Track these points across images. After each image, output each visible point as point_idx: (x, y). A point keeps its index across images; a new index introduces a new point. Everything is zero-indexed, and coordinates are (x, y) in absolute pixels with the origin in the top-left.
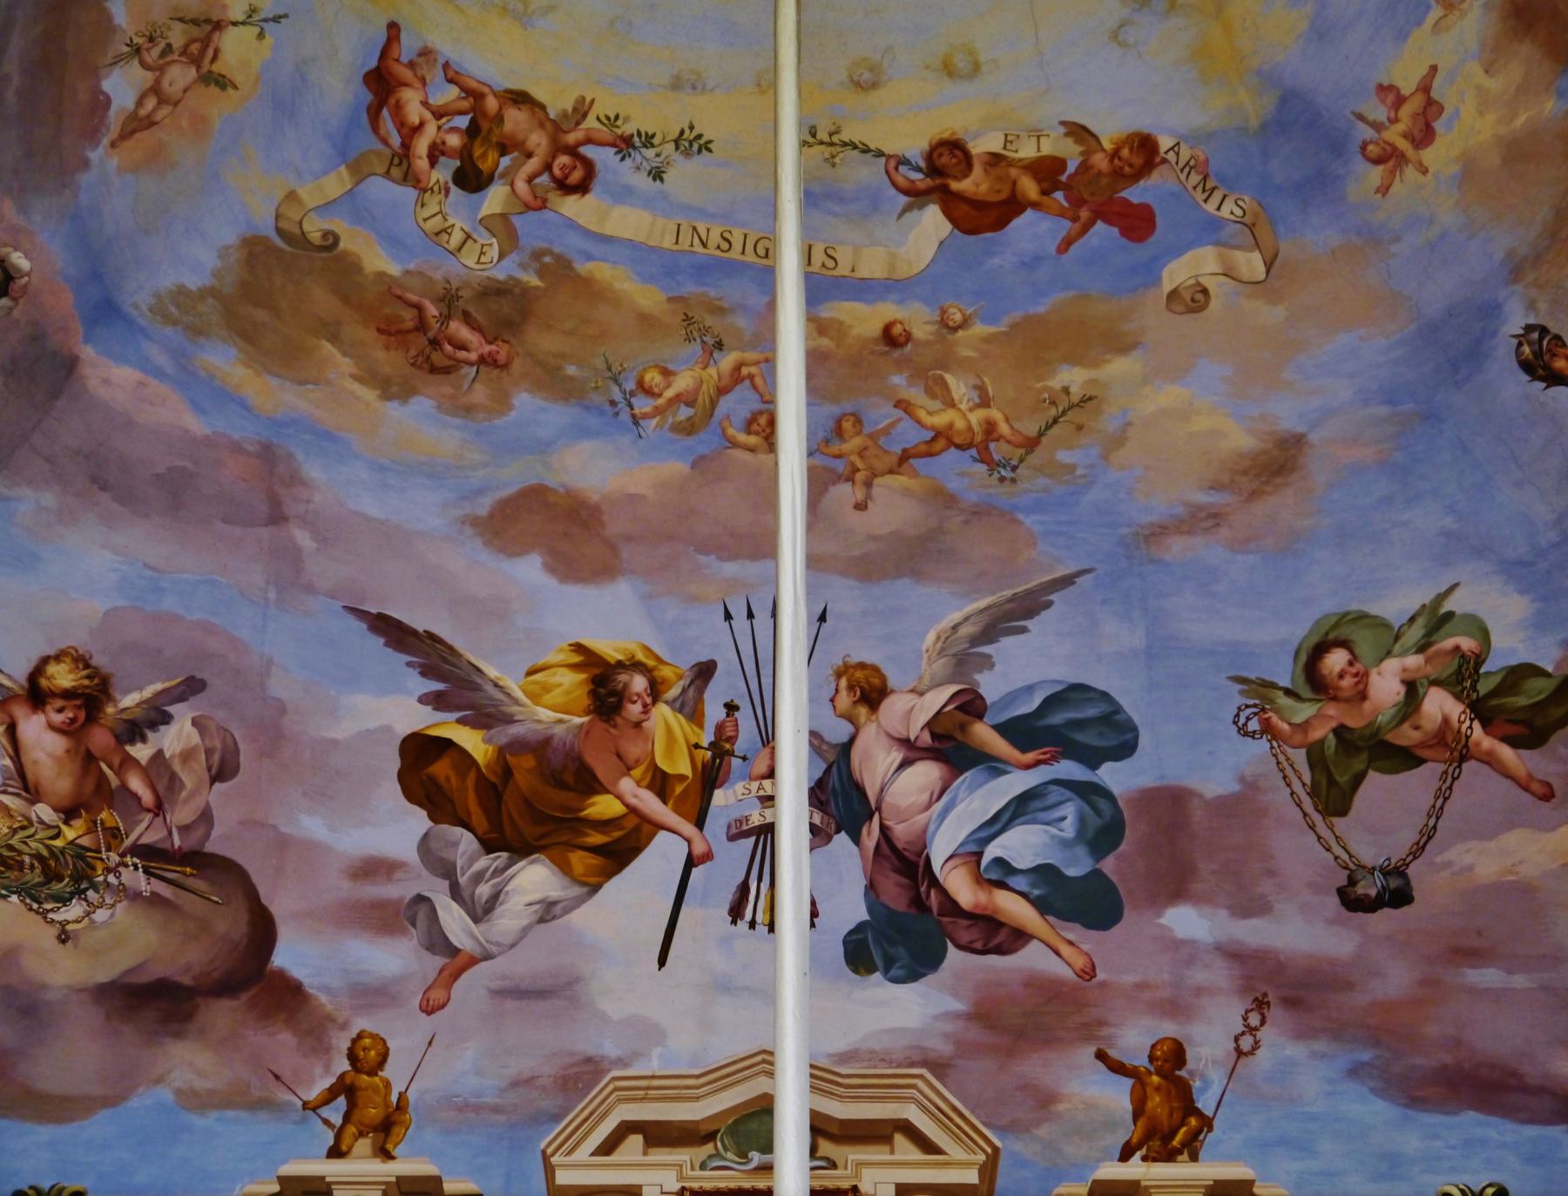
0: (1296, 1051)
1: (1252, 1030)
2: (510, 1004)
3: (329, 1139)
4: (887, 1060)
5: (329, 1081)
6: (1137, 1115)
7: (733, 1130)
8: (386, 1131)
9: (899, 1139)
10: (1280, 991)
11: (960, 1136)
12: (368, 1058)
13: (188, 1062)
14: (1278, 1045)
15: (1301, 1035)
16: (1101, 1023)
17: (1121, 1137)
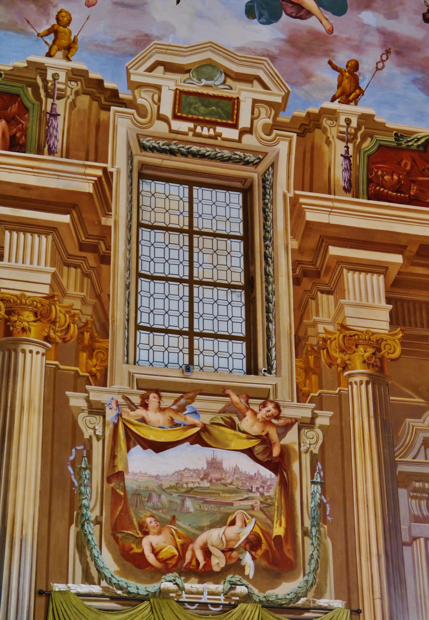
0: (396, 71)
1: (383, 61)
2: (120, 9)
3: (47, 50)
4: (254, 53)
5: (48, 27)
6: (339, 85)
7: (197, 70)
8: (69, 49)
9: (255, 82)
10: (395, 48)
11: (277, 84)
12: (63, 20)
15: (400, 65)
16: (332, 51)
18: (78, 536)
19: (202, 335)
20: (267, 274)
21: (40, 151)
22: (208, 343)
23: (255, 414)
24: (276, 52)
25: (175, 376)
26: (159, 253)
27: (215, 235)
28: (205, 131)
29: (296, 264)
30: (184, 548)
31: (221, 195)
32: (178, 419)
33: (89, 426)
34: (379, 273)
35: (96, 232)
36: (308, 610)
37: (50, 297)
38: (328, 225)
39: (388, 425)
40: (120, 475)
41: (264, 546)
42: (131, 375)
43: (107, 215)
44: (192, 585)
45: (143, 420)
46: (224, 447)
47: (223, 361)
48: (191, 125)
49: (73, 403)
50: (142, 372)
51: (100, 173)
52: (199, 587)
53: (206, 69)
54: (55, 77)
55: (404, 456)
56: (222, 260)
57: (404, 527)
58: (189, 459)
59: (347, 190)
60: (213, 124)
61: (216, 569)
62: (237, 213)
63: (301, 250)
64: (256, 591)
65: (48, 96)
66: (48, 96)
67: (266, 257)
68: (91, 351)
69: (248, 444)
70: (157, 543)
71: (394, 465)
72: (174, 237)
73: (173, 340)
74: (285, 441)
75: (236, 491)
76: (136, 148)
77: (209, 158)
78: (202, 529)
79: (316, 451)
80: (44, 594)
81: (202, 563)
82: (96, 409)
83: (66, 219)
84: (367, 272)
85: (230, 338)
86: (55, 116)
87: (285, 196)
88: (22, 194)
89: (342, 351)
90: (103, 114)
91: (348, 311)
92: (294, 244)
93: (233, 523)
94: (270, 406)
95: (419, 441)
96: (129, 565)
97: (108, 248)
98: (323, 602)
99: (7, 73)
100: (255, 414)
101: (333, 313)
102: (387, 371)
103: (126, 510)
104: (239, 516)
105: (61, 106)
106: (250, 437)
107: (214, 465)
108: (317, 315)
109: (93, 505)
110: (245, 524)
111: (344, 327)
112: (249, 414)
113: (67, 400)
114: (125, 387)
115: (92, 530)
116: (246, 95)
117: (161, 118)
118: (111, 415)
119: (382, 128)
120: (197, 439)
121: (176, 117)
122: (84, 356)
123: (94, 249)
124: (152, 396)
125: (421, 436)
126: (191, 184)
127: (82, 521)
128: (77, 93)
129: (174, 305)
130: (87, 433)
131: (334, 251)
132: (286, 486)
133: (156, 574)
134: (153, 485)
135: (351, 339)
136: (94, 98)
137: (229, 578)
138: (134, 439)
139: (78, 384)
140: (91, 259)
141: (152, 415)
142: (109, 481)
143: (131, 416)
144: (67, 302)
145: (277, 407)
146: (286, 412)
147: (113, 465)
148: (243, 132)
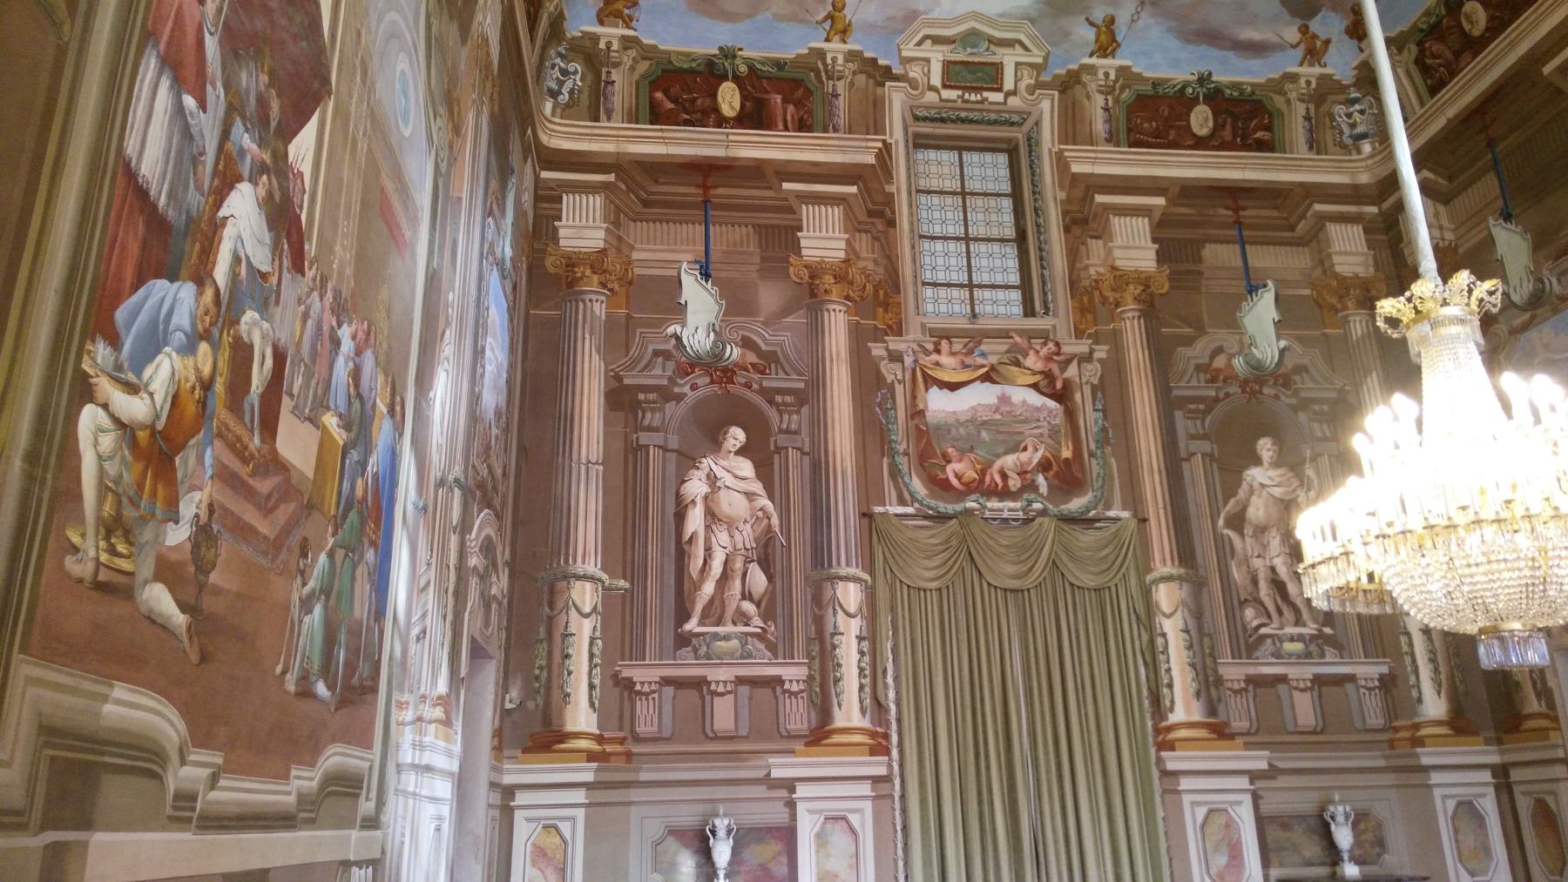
0: (1151, 21)
8: (844, 33)
11: (1039, 47)
14: (1146, 20)
17: (1090, 49)
18: (890, 466)
19: (980, 286)
20: (1038, 226)
21: (825, 130)
22: (987, 294)
24: (1034, 14)
25: (964, 324)
26: (937, 215)
27: (985, 195)
28: (973, 97)
29: (1065, 213)
30: (983, 473)
31: (988, 157)
32: (968, 361)
33: (890, 371)
35: (879, 198)
36: (1099, 520)
37: (846, 261)
38: (1092, 175)
39: (1161, 355)
40: (922, 413)
41: (1055, 468)
42: (923, 326)
44: (994, 504)
45: (937, 364)
46: (1010, 382)
47: (1004, 307)
48: (960, 93)
49: (875, 352)
50: (933, 322)
51: (880, 145)
52: (1000, 505)
53: (971, 38)
54: (834, 59)
55: (1180, 380)
56: (994, 217)
57: (1182, 445)
59: (1108, 141)
61: (1013, 489)
62: (1004, 172)
63: (1068, 201)
65: (830, 78)
67: (1036, 210)
68: (886, 306)
70: (958, 469)
72: (949, 200)
73: (955, 293)
74: (1067, 374)
75: (1026, 421)
76: (910, 119)
78: (998, 456)
79: (1096, 382)
80: (867, 515)
81: (1000, 485)
82: (896, 357)
83: (853, 189)
85: (1007, 287)
86: (836, 96)
88: (814, 170)
89: (1114, 290)
90: (879, 90)
91: (1117, 253)
92: (1062, 195)
93: (1025, 449)
94: (1051, 345)
95: (1191, 368)
97: (893, 213)
98: (1112, 514)
99: (792, 61)
100: (1037, 352)
103: (929, 443)
104: (1029, 442)
105: (841, 86)
106: (1034, 373)
107: (1004, 399)
110: (1036, 450)
111: (1114, 268)
112: (1032, 353)
113: (869, 351)
114: (919, 336)
115: (902, 462)
116: (1009, 60)
117: (932, 88)
118: (908, 361)
119: (1139, 78)
120: (987, 378)
121: (945, 86)
122: (881, 310)
123: (881, 214)
124: (944, 342)
125: (1193, 362)
126: (960, 150)
127: (892, 453)
128: (854, 73)
129: (953, 261)
130: (890, 378)
131: (1100, 198)
132: (1070, 414)
134: (951, 420)
135: (1121, 279)
136: (870, 76)
137: (1025, 496)
138: (930, 381)
139: (878, 335)
140: (878, 222)
141: (945, 359)
142: (913, 417)
143: (927, 360)
144: (861, 264)
145: (1057, 344)
146: (1066, 349)
147: (914, 405)
148: (1008, 94)
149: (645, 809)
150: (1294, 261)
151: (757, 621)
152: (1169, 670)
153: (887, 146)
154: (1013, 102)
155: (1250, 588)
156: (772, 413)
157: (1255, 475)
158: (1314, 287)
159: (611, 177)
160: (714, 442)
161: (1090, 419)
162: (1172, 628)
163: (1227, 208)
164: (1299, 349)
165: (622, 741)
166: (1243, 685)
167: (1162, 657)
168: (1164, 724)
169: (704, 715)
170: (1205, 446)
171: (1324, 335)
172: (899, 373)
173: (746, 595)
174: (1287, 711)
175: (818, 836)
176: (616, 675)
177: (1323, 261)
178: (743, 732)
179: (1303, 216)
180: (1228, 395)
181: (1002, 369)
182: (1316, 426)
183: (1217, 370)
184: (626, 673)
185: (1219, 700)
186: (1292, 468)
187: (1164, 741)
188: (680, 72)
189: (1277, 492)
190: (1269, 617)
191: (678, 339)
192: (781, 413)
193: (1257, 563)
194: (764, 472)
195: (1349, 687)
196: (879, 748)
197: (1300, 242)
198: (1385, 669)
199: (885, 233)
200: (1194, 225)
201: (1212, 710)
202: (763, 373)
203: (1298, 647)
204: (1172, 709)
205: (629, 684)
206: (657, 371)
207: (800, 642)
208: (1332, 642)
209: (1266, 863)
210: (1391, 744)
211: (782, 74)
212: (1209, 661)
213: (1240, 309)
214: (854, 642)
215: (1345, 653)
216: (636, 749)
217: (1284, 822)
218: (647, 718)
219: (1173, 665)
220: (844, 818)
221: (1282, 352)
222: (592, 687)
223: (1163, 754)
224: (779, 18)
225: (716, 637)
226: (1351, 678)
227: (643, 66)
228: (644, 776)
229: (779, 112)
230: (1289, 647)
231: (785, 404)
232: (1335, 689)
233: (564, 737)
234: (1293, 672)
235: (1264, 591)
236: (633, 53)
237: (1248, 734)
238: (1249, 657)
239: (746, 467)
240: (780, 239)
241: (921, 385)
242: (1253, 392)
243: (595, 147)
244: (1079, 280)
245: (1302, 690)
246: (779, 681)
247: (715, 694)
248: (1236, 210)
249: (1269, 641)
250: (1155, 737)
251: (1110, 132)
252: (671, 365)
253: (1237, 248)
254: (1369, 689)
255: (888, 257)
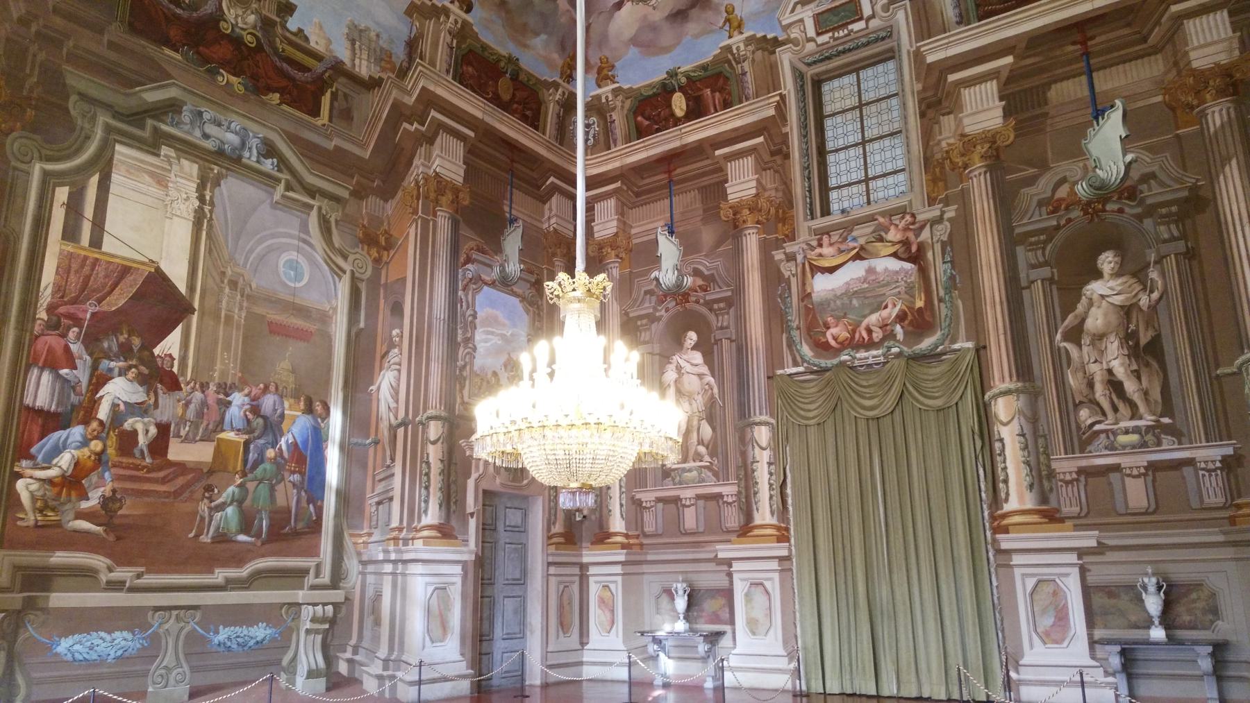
12: (730, 10)
13: (692, 27)
21: (741, 102)
22: (880, 183)
23: (897, 226)
28: (841, 33)
29: (920, 102)
30: (854, 331)
31: (880, 68)
32: (843, 247)
33: (787, 269)
34: (992, 79)
37: (757, 195)
39: (1004, 200)
40: (809, 295)
42: (809, 228)
43: (785, 125)
44: (862, 354)
45: (820, 255)
46: (876, 256)
48: (830, 34)
49: (777, 258)
51: (778, 98)
52: (866, 354)
54: (738, 49)
55: (1022, 219)
57: (1023, 275)
58: (853, 272)
59: (959, 23)
60: (845, 25)
63: (924, 89)
64: (905, 349)
65: (738, 63)
66: (738, 63)
69: (892, 250)
71: (1013, 229)
75: (888, 284)
77: (854, 49)
78: (865, 317)
79: (945, 238)
82: (791, 258)
83: (761, 139)
84: (981, 83)
86: (744, 74)
87: (909, 52)
89: (963, 155)
90: (772, 57)
91: (966, 121)
92: (918, 87)
93: (886, 307)
94: (908, 218)
96: (820, 350)
97: (788, 148)
98: (956, 346)
100: (897, 226)
101: (953, 127)
102: (1002, 157)
103: (814, 317)
104: (889, 301)
106: (894, 243)
107: (871, 271)
108: (940, 133)
109: (795, 319)
110: (895, 305)
111: (963, 135)
112: (892, 228)
114: (808, 237)
115: (795, 333)
118: (800, 258)
120: (858, 257)
121: (818, 34)
122: (780, 225)
123: (779, 152)
130: (787, 274)
131: (952, 78)
132: (923, 272)
133: (837, 352)
134: (830, 296)
135: (968, 143)
136: (764, 50)
138: (816, 269)
139: (778, 244)
140: (778, 159)
143: (812, 255)
144: (767, 194)
145: (913, 216)
146: (920, 218)
147: (805, 290)
149: (651, 577)
150: (1143, 74)
151: (707, 458)
152: (1005, 469)
153: (782, 97)
154: (874, 23)
155: (1085, 391)
156: (712, 317)
157: (1096, 288)
158: (1166, 91)
159: (618, 184)
160: (679, 343)
161: (940, 270)
162: (1009, 435)
163: (1074, 43)
164: (1146, 157)
165: (637, 537)
166: (1075, 476)
167: (999, 458)
168: (999, 512)
169: (679, 519)
170: (1046, 272)
171: (1177, 136)
172: (793, 269)
173: (701, 442)
174: (1119, 497)
175: (747, 595)
176: (633, 497)
177: (1179, 62)
178: (701, 530)
179: (1158, 23)
180: (1069, 220)
181: (869, 247)
182: (1162, 228)
183: (1061, 200)
184: (638, 496)
185: (1051, 490)
186: (1134, 275)
187: (999, 526)
188: (649, 97)
189: (1118, 300)
190: (1104, 414)
191: (657, 279)
192: (717, 315)
193: (1094, 368)
194: (708, 360)
195: (1187, 471)
196: (783, 537)
197: (1155, 50)
198: (1230, 451)
199: (782, 166)
200: (1042, 70)
201: (1044, 499)
202: (706, 290)
203: (1134, 438)
204: (1007, 500)
205: (639, 503)
206: (647, 305)
207: (732, 470)
208: (1172, 431)
209: (1090, 624)
210: (1232, 521)
211: (708, 73)
212: (1042, 458)
213: (1085, 137)
214: (766, 466)
215: (1184, 439)
216: (645, 541)
217: (1110, 591)
218: (651, 522)
219: (1008, 464)
220: (762, 584)
221: (1128, 166)
222: (621, 505)
223: (998, 536)
224: (697, 36)
225: (684, 470)
226: (1190, 462)
227: (628, 103)
228: (650, 558)
229: (710, 101)
230: (1122, 439)
231: (720, 309)
232: (1172, 474)
233: (610, 535)
234: (1125, 461)
235: (1100, 392)
236: (620, 98)
237: (1079, 517)
238: (1082, 451)
239: (697, 357)
240: (716, 191)
241: (809, 274)
242: (1096, 212)
243: (609, 167)
244: (933, 156)
245: (1134, 477)
246: (720, 496)
247: (684, 506)
248: (1084, 43)
249: (1103, 436)
250: (991, 523)
251: (961, 15)
252: (654, 298)
253: (1084, 79)
254: (1209, 471)
255: (785, 183)
